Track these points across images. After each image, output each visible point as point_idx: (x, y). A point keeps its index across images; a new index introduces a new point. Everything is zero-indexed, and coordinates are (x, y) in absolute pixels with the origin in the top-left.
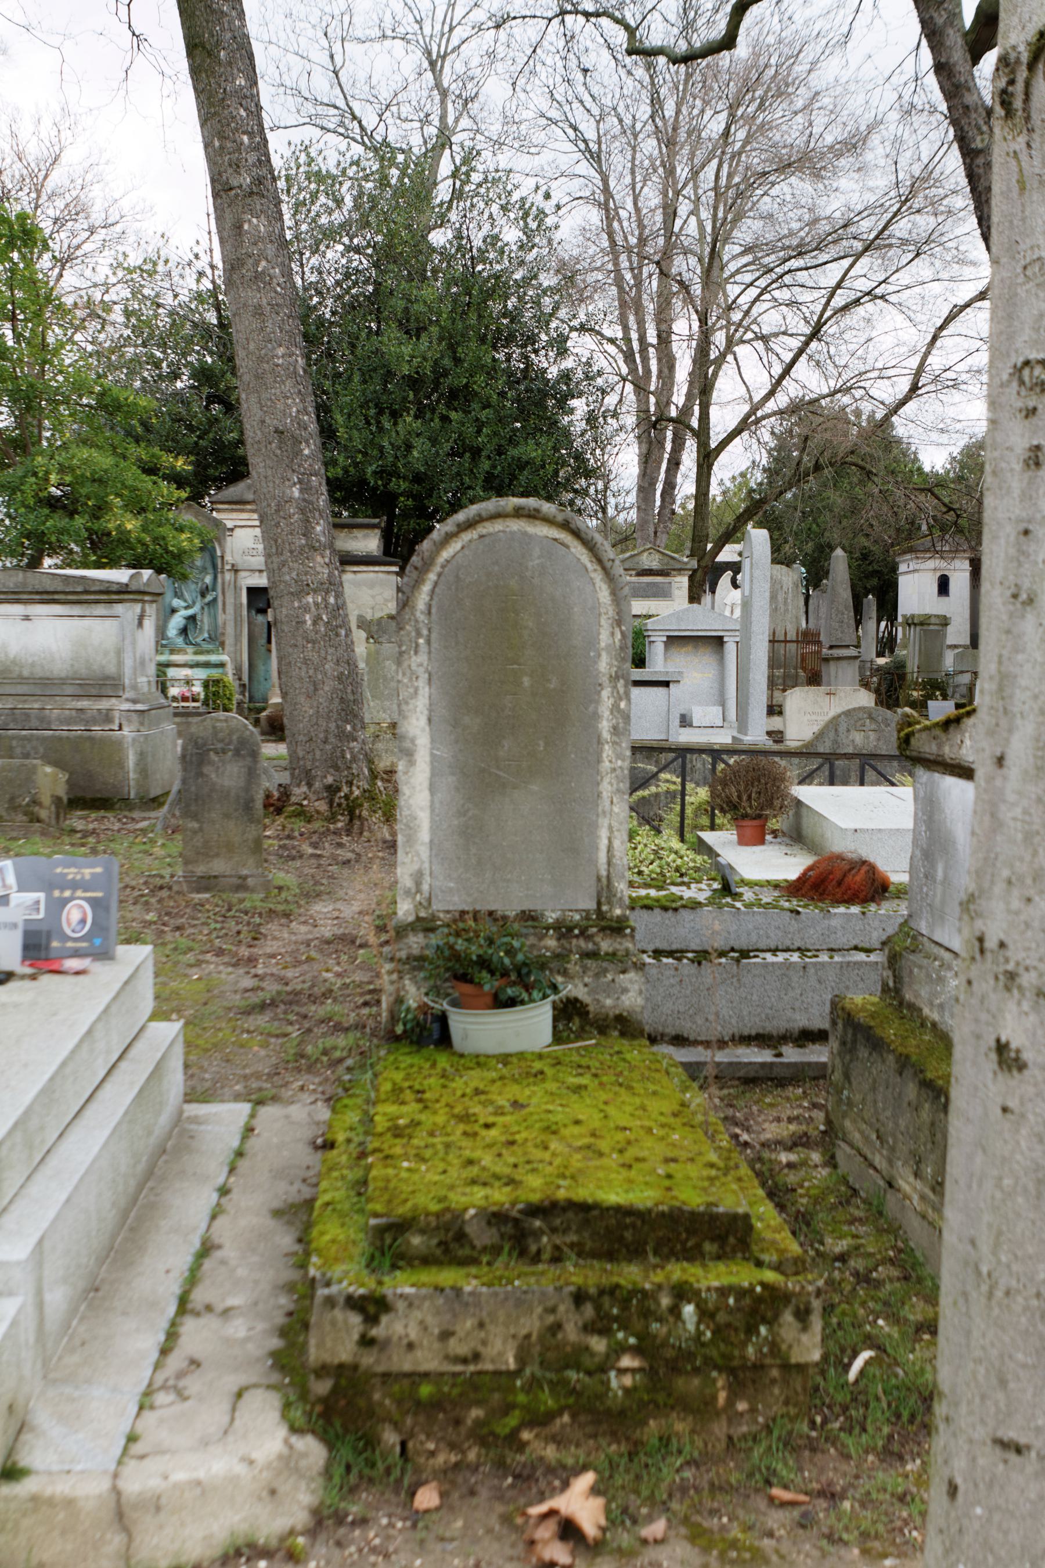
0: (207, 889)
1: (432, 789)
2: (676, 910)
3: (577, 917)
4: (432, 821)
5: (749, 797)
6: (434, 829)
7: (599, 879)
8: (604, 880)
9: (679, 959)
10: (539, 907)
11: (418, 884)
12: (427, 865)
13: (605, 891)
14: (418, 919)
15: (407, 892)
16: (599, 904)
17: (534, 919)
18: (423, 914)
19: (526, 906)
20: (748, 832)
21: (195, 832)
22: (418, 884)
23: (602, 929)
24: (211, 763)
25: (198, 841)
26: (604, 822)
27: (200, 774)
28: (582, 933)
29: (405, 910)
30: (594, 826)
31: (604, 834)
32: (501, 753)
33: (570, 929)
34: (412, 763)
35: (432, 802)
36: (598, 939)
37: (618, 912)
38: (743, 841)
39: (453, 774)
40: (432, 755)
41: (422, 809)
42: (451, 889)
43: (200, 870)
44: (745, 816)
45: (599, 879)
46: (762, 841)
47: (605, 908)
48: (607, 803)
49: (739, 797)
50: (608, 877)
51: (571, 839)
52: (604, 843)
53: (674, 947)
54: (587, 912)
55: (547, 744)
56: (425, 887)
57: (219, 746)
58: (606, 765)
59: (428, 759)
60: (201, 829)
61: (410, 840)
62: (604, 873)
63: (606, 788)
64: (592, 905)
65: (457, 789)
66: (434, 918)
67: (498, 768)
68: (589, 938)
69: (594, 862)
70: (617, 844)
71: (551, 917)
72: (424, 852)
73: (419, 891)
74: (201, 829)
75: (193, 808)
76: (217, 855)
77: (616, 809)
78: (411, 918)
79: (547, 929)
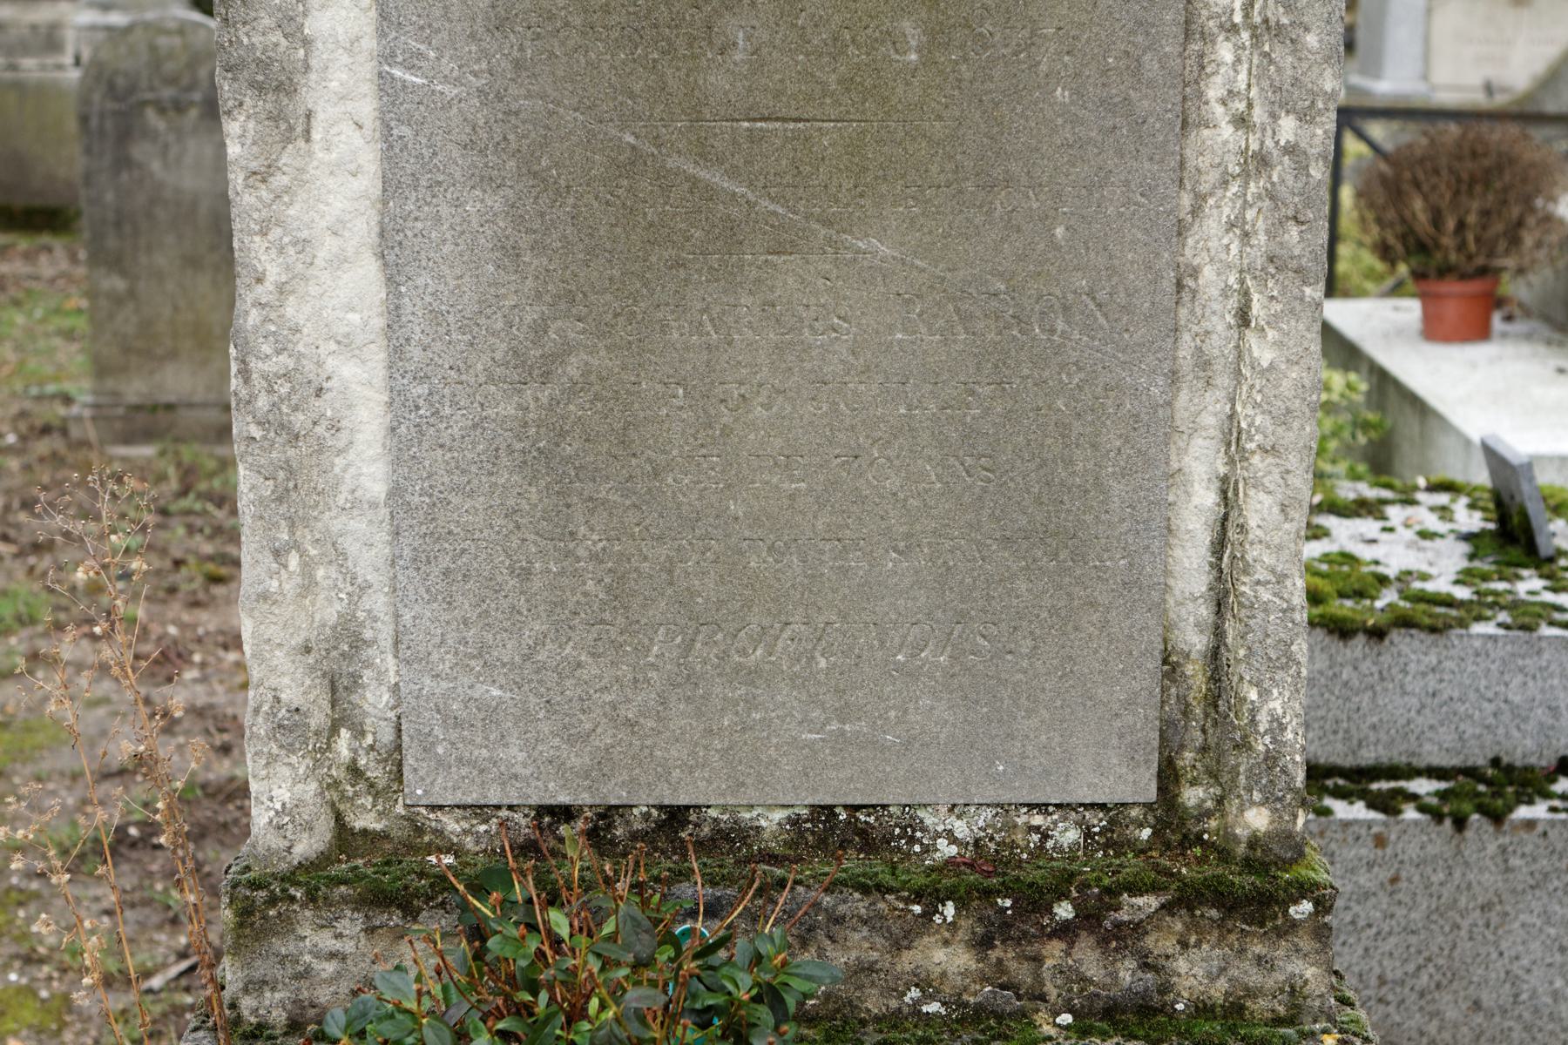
0: (147, 436)
1: (392, 246)
2: (1377, 634)
3: (1069, 836)
4: (398, 401)
5: (1461, 226)
6: (404, 446)
7: (1171, 666)
8: (1195, 674)
9: (1387, 804)
10: (893, 795)
11: (340, 688)
12: (378, 601)
13: (1198, 715)
14: (345, 838)
15: (290, 728)
16: (1168, 776)
17: (868, 841)
18: (365, 819)
19: (841, 787)
20: (1451, 311)
21: (118, 300)
22: (340, 688)
23: (1185, 900)
24: (149, 134)
25: (127, 320)
26: (1202, 411)
27: (123, 162)
28: (1088, 919)
29: (283, 804)
30: (1157, 430)
31: (1200, 462)
32: (717, 81)
33: (1035, 900)
34: (288, 125)
35: (394, 312)
36: (1160, 943)
37: (1258, 819)
38: (1434, 330)
39: (487, 181)
40: (384, 82)
41: (345, 344)
42: (491, 713)
43: (135, 389)
44: (1445, 271)
45: (1171, 666)
46: (1480, 332)
47: (1192, 796)
48: (1220, 321)
49: (1437, 220)
50: (1215, 655)
51: (1043, 497)
52: (1198, 504)
53: (1367, 757)
54: (1114, 811)
55: (936, 38)
56: (375, 701)
57: (167, 93)
58: (1221, 137)
59: (367, 108)
60: (132, 293)
61: (293, 491)
62: (1195, 641)
63: (1216, 250)
64: (1141, 786)
65: (510, 253)
66: (417, 837)
67: (704, 155)
68: (1122, 938)
69: (1144, 587)
70: (1259, 509)
71: (950, 833)
72: (367, 544)
73: (343, 718)
74: (132, 293)
75: (112, 242)
76: (173, 355)
77: (1262, 352)
78: (306, 847)
79: (931, 897)
